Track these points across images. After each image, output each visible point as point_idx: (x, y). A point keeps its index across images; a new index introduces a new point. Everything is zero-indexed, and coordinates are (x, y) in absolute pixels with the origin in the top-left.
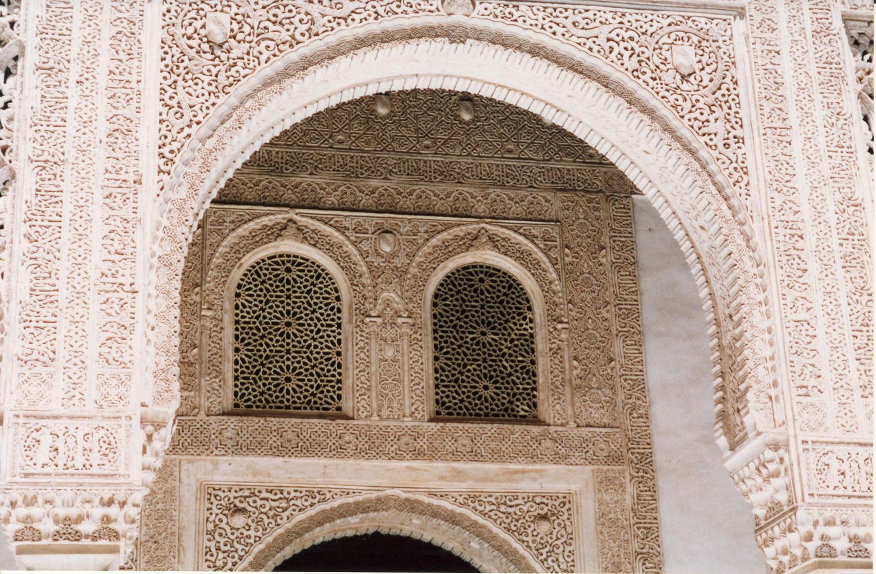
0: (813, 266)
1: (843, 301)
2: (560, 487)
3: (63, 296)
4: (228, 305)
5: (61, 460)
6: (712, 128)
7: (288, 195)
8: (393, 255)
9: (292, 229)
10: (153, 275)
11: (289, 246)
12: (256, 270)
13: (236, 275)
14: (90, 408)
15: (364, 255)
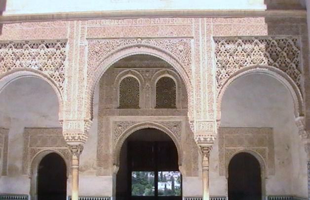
0: (202, 88)
2: (179, 120)
3: (72, 100)
4: (119, 87)
5: (72, 127)
6: (186, 61)
7: (129, 65)
8: (149, 76)
9: (130, 72)
10: (86, 96)
11: (130, 75)
12: (124, 80)
13: (120, 82)
14: (76, 119)
15: (143, 76)
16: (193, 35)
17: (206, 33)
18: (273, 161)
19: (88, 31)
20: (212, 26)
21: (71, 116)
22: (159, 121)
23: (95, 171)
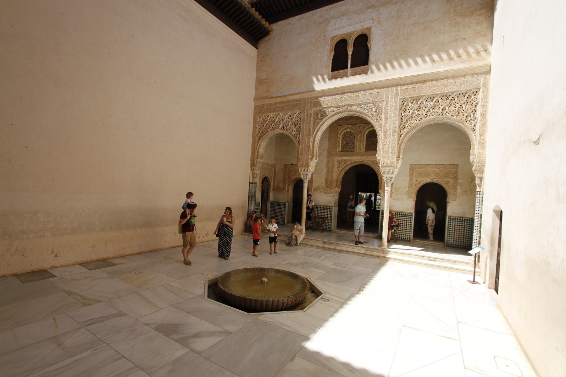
0: (388, 137)
1: (391, 141)
4: (341, 138)
6: (377, 119)
8: (361, 130)
11: (348, 130)
12: (344, 134)
13: (342, 134)
16: (384, 99)
17: (394, 97)
18: (456, 191)
19: (314, 104)
20: (399, 91)
21: (303, 157)
22: (366, 160)
23: (324, 190)
